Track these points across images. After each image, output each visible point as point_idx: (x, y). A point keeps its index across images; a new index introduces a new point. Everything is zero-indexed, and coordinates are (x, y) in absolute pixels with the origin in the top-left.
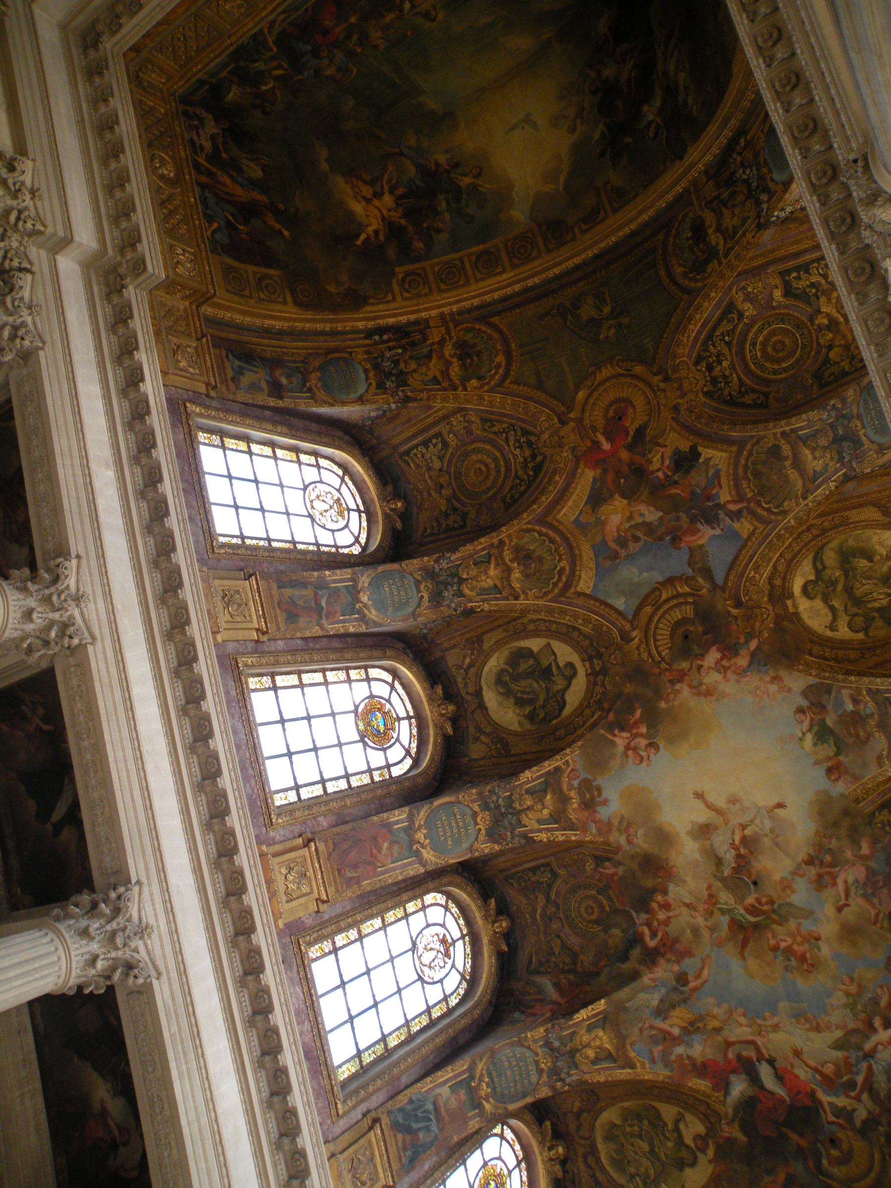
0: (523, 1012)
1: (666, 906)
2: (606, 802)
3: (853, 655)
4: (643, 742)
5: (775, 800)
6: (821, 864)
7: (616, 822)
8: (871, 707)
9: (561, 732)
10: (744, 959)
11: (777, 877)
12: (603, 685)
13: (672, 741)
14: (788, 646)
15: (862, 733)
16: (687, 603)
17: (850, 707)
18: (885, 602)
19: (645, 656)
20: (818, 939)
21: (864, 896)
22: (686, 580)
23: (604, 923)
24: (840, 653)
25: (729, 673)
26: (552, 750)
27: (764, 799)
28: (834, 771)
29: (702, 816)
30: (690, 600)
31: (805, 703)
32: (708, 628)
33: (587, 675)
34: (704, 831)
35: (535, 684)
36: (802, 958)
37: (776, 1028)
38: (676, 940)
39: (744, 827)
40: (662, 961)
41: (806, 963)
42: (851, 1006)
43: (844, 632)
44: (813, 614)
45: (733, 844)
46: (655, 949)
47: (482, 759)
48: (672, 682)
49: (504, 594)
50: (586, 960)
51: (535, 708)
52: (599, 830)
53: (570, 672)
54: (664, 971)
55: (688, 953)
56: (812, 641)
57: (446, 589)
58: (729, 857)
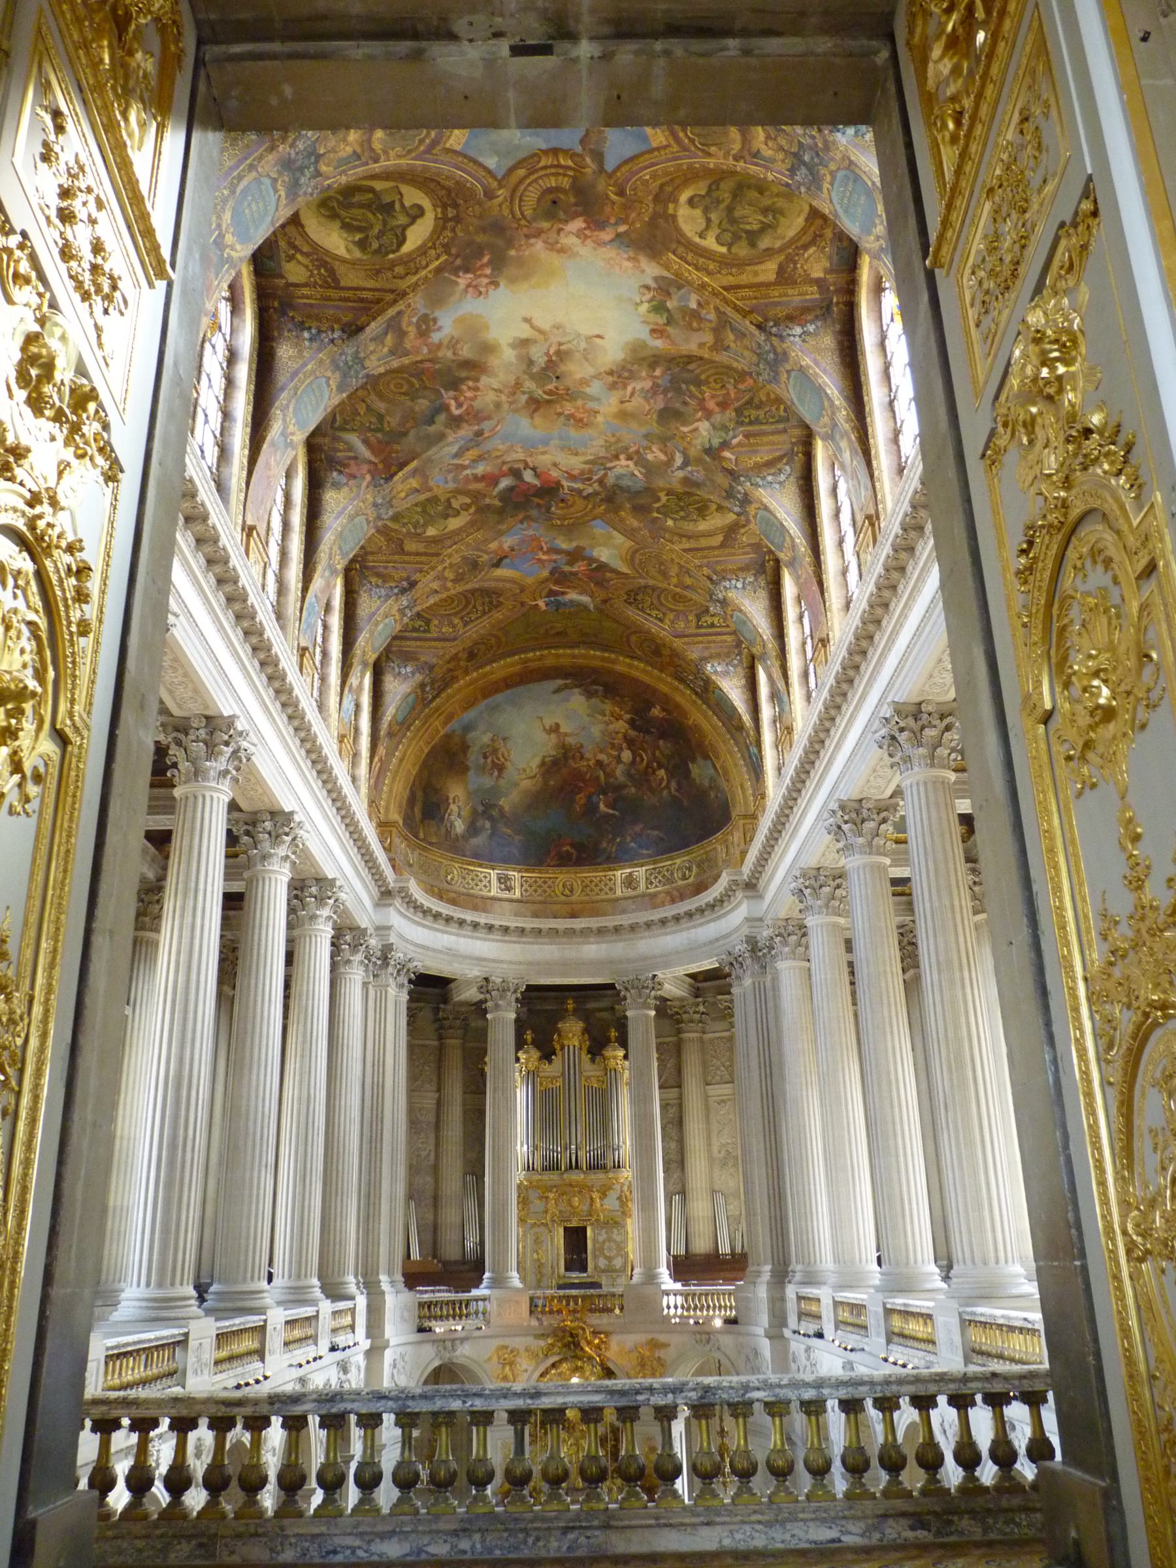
0: (340, 472)
1: (476, 389)
2: (439, 329)
3: (712, 266)
4: (485, 281)
5: (597, 332)
6: (619, 376)
7: (445, 342)
8: (712, 316)
9: (399, 270)
11: (578, 376)
12: (453, 230)
13: (512, 281)
14: (655, 238)
16: (565, 175)
17: (694, 305)
18: (756, 227)
19: (506, 212)
20: (597, 412)
21: (647, 399)
22: (573, 155)
23: (413, 395)
24: (701, 260)
25: (588, 241)
26: (392, 291)
27: (586, 330)
28: (656, 332)
29: (525, 332)
30: (571, 173)
31: (653, 285)
32: (579, 200)
33: (436, 218)
34: (524, 343)
35: (370, 216)
36: (581, 420)
37: (544, 453)
38: (478, 412)
39: (560, 344)
40: (465, 425)
41: (580, 423)
42: (607, 448)
43: (710, 243)
44: (688, 220)
45: (547, 354)
47: (306, 285)
48: (527, 237)
49: (364, 159)
50: (393, 421)
51: (367, 237)
52: (430, 351)
53: (417, 213)
54: (466, 431)
55: (489, 418)
56: (679, 242)
57: (303, 174)
58: (541, 361)
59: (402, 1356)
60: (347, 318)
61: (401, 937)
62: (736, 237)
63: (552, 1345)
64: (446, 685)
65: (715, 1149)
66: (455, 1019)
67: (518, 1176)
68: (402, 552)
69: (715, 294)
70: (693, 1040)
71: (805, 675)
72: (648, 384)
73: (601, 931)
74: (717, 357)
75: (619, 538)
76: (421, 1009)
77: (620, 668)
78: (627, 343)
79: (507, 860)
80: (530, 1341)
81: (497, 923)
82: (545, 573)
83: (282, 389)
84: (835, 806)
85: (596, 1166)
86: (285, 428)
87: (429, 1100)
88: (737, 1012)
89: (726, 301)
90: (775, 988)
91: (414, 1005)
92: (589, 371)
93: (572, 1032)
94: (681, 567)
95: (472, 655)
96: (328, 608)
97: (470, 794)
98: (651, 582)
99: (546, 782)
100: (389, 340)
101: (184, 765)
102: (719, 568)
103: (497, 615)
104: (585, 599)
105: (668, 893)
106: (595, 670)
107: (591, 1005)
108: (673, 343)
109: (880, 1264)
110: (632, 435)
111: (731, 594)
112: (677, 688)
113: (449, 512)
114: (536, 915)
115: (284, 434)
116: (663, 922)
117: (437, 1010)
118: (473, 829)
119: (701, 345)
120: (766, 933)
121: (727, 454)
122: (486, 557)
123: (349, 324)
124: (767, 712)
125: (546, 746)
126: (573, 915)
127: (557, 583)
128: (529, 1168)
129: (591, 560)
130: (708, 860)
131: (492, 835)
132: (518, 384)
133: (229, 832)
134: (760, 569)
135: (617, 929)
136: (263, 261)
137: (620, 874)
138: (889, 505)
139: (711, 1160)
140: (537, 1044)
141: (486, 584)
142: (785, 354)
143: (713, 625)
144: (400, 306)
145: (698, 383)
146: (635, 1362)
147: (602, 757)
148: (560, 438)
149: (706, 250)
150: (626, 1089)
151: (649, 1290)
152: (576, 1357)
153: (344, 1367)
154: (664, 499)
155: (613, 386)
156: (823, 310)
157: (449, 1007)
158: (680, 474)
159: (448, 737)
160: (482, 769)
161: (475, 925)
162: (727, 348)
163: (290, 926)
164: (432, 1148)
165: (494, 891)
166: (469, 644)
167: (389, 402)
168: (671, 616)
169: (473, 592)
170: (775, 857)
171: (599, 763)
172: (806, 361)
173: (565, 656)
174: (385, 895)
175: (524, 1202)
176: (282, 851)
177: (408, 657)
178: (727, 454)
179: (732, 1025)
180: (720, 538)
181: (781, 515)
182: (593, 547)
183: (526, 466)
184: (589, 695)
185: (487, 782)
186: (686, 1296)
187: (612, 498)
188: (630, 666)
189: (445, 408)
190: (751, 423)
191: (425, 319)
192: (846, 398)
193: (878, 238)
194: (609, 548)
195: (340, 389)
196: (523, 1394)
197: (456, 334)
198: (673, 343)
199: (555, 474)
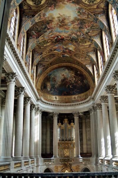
1: (52, 24)
2: (46, 15)
3: (87, 6)
4: (53, 8)
6: (73, 22)
8: (87, 13)
10: (60, 28)
13: (57, 8)
15: (84, 14)
17: (84, 12)
20: (69, 27)
23: (42, 25)
27: (68, 15)
29: (59, 16)
34: (59, 17)
41: (67, 29)
42: (71, 33)
43: (87, 2)
46: (49, 28)
50: (39, 29)
54: (50, 30)
55: (53, 28)
58: (61, 20)
59: (41, 167)
60: (32, 14)
61: (40, 106)
62: (90, 2)
64: (47, 69)
65: (87, 138)
67: (58, 141)
68: (41, 49)
69: (87, 10)
71: (101, 67)
72: (77, 23)
73: (70, 105)
74: (88, 19)
75: (73, 46)
77: (73, 66)
78: (74, 17)
79: (56, 95)
81: (55, 104)
82: (62, 51)
83: (23, 24)
84: (106, 86)
85: (70, 140)
86: (23, 30)
87: (45, 130)
89: (89, 11)
90: (97, 114)
92: (69, 21)
93: (66, 121)
94: (82, 51)
95: (51, 64)
96: (29, 57)
97: (51, 85)
98: (78, 53)
99: (62, 83)
100: (39, 17)
101: (8, 80)
102: (88, 51)
103: (55, 58)
104: (68, 55)
105: (80, 100)
106: (69, 66)
107: (69, 116)
108: (81, 17)
109: (112, 154)
110: (75, 31)
111: (90, 55)
112: (82, 69)
113: (48, 42)
114: (60, 103)
115: (23, 31)
116: (80, 104)
117: (46, 117)
118: (51, 90)
119: (85, 17)
120: (95, 105)
121: (89, 34)
122: (53, 49)
123: (33, 15)
124: (96, 72)
125: (62, 78)
126: (66, 103)
127: (64, 53)
128: (60, 140)
129: (69, 49)
130: (86, 95)
131: (54, 91)
132: (58, 23)
133: (15, 90)
134: (94, 51)
135: (73, 105)
136: (21, 6)
137: (73, 97)
138: (114, 41)
139: (87, 139)
140: (61, 122)
141: (53, 53)
142: (98, 19)
143: (87, 59)
144: (40, 12)
145: (85, 23)
147: (70, 79)
148: (64, 31)
149: (86, 4)
150: (74, 129)
151: (78, 158)
153: (33, 168)
154: (80, 40)
155: (72, 24)
156: (103, 12)
157: (48, 117)
158: (82, 36)
159: (47, 76)
160: (52, 81)
161: (51, 104)
162: (89, 18)
163: (24, 104)
164: (45, 137)
165: (54, 99)
166: (50, 62)
167: (39, 26)
168: (81, 58)
169: (51, 54)
170: (97, 94)
171: (70, 80)
172: (101, 20)
173: (65, 64)
174: (38, 100)
175: (59, 145)
176: (23, 93)
177: (41, 64)
178: (89, 34)
179: (90, 119)
180: (88, 46)
181: (97, 42)
182: (69, 48)
183: (59, 36)
184: (68, 70)
185: (53, 83)
186: (83, 159)
187: (72, 40)
188: (75, 66)
189: (47, 27)
190: (93, 29)
191: (44, 14)
192: (107, 25)
193: (112, 2)
194: (71, 48)
195: (31, 24)
196: (60, 174)
197: (49, 16)
198: (81, 17)
199: (63, 37)
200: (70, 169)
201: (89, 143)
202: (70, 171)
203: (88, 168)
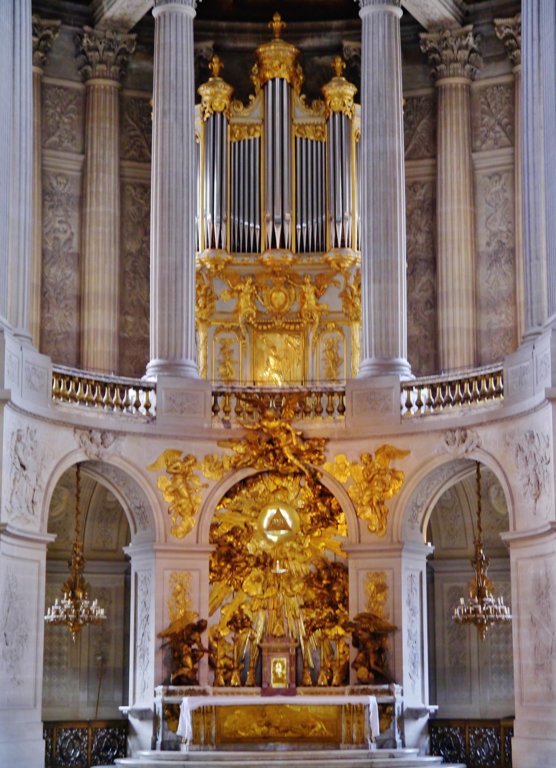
63: (245, 455)
66: (110, 49)
70: (456, 88)
76: (56, 30)
80: (212, 447)
87: (68, 163)
88: (525, 40)
91: (45, 22)
139: (477, 256)
140: (227, 76)
146: (359, 478)
151: (384, 381)
152: (275, 473)
157: (98, 32)
164: (75, 229)
179: (515, 62)
186: (433, 388)
200: (309, 493)
201: (494, 281)
202: (311, 506)
203: (476, 456)
